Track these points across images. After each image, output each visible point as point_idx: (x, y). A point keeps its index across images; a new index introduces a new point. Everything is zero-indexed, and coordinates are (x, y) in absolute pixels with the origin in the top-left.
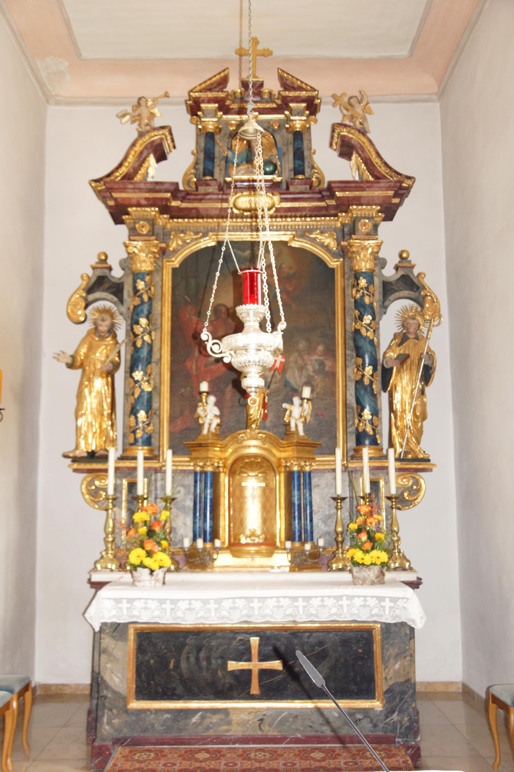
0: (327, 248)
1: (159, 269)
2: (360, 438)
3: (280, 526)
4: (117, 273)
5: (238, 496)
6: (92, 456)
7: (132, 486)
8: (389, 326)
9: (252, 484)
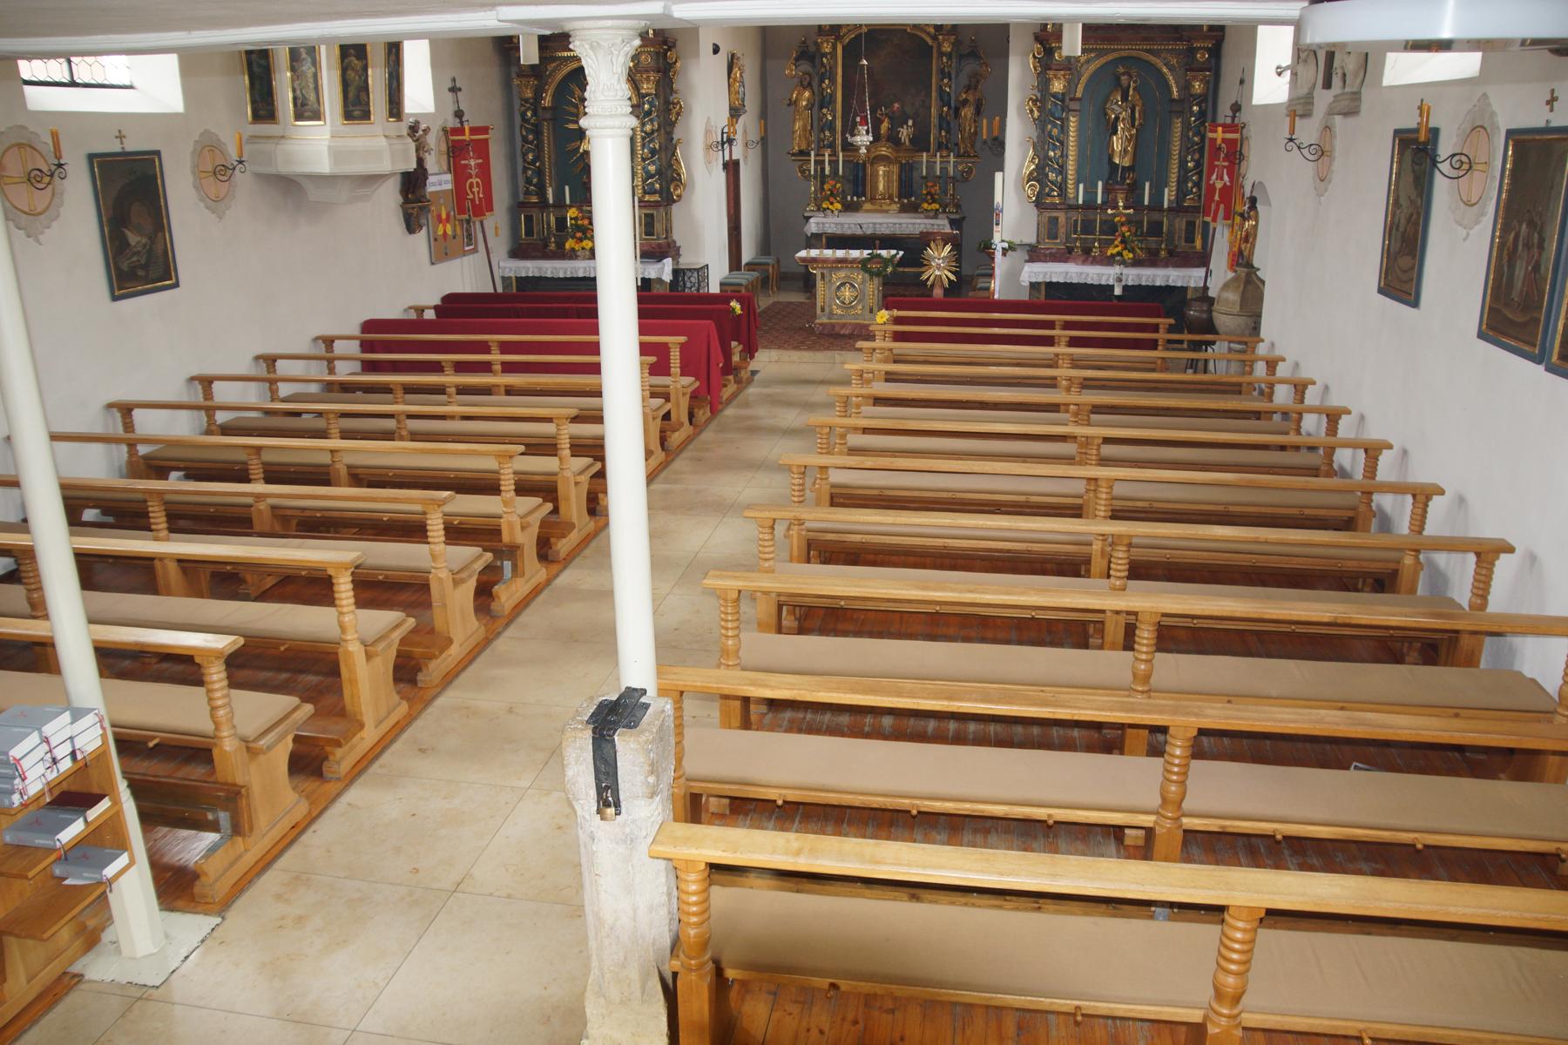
0: (928, 34)
1: (834, 47)
2: (940, 147)
3: (895, 191)
4: (812, 49)
5: (875, 175)
6: (801, 153)
7: (823, 169)
8: (964, 80)
9: (881, 170)
